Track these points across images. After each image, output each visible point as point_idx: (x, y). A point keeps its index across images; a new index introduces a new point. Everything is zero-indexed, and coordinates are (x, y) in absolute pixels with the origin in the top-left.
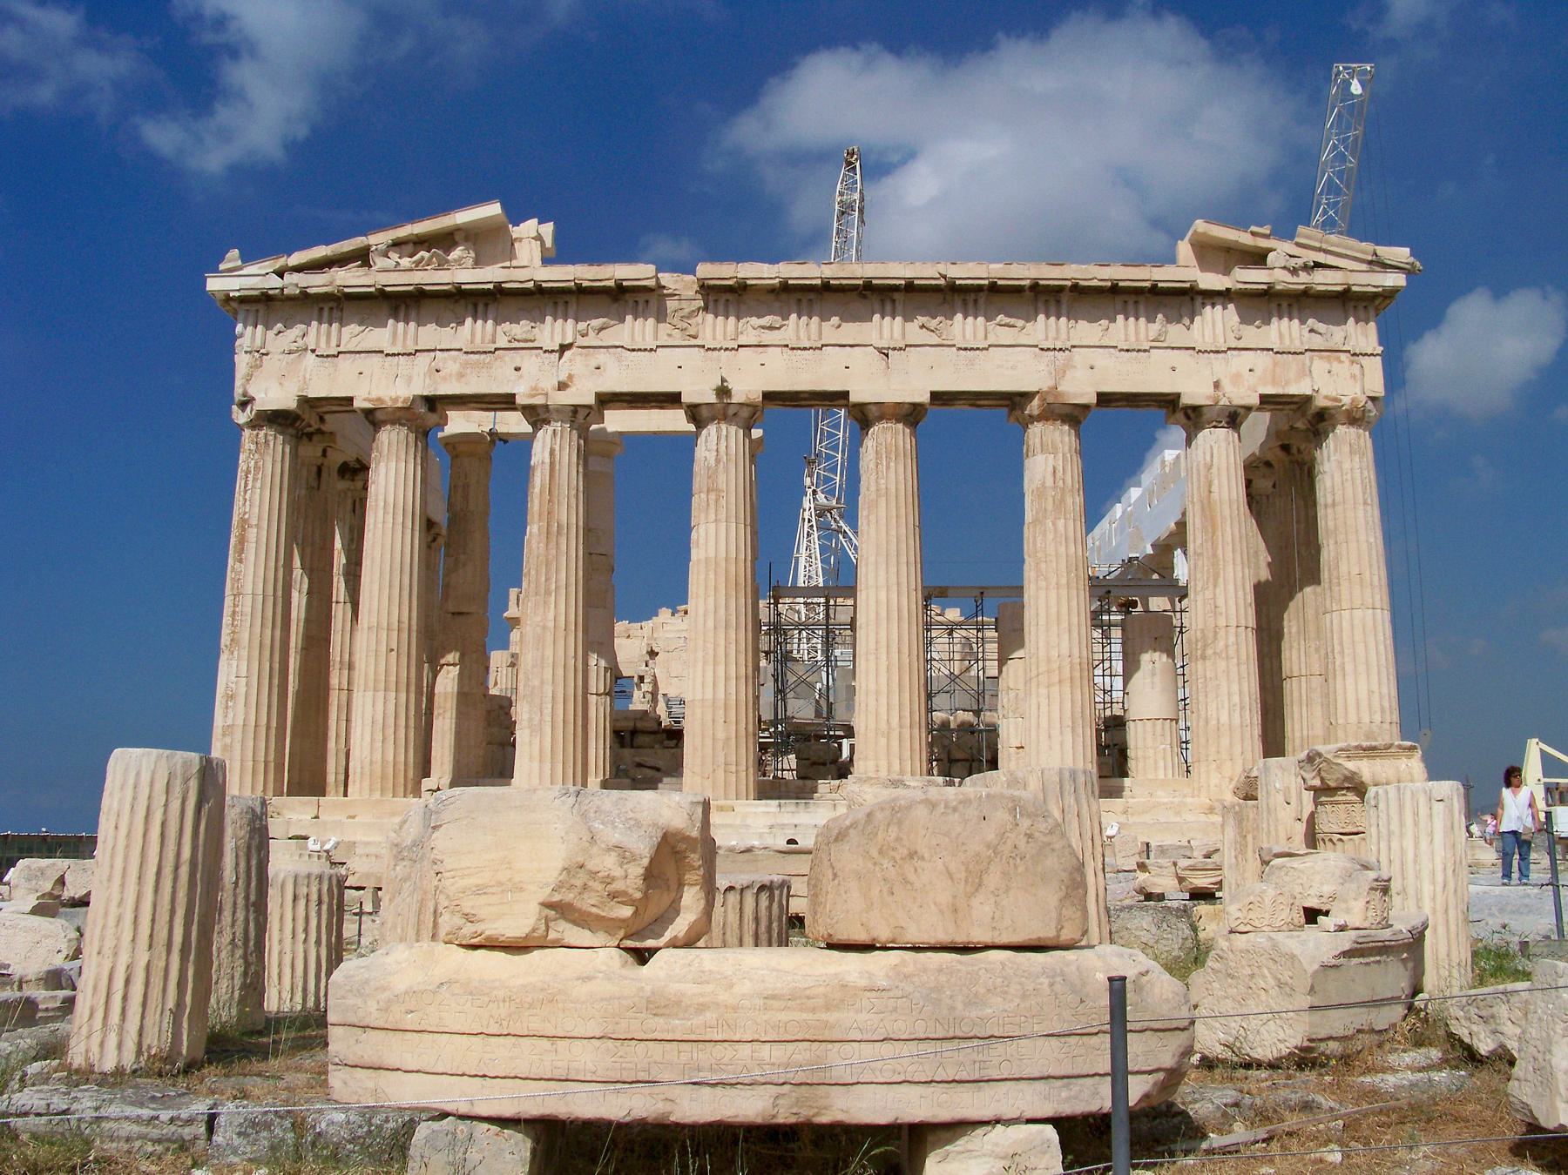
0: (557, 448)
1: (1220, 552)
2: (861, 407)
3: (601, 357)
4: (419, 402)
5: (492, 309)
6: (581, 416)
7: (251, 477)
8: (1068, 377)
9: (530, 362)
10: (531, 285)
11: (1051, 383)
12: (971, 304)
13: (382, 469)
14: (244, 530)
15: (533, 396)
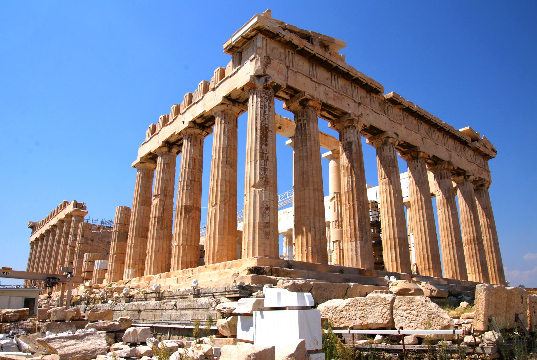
3: (368, 111)
9: (352, 105)
13: (311, 124)
15: (355, 116)
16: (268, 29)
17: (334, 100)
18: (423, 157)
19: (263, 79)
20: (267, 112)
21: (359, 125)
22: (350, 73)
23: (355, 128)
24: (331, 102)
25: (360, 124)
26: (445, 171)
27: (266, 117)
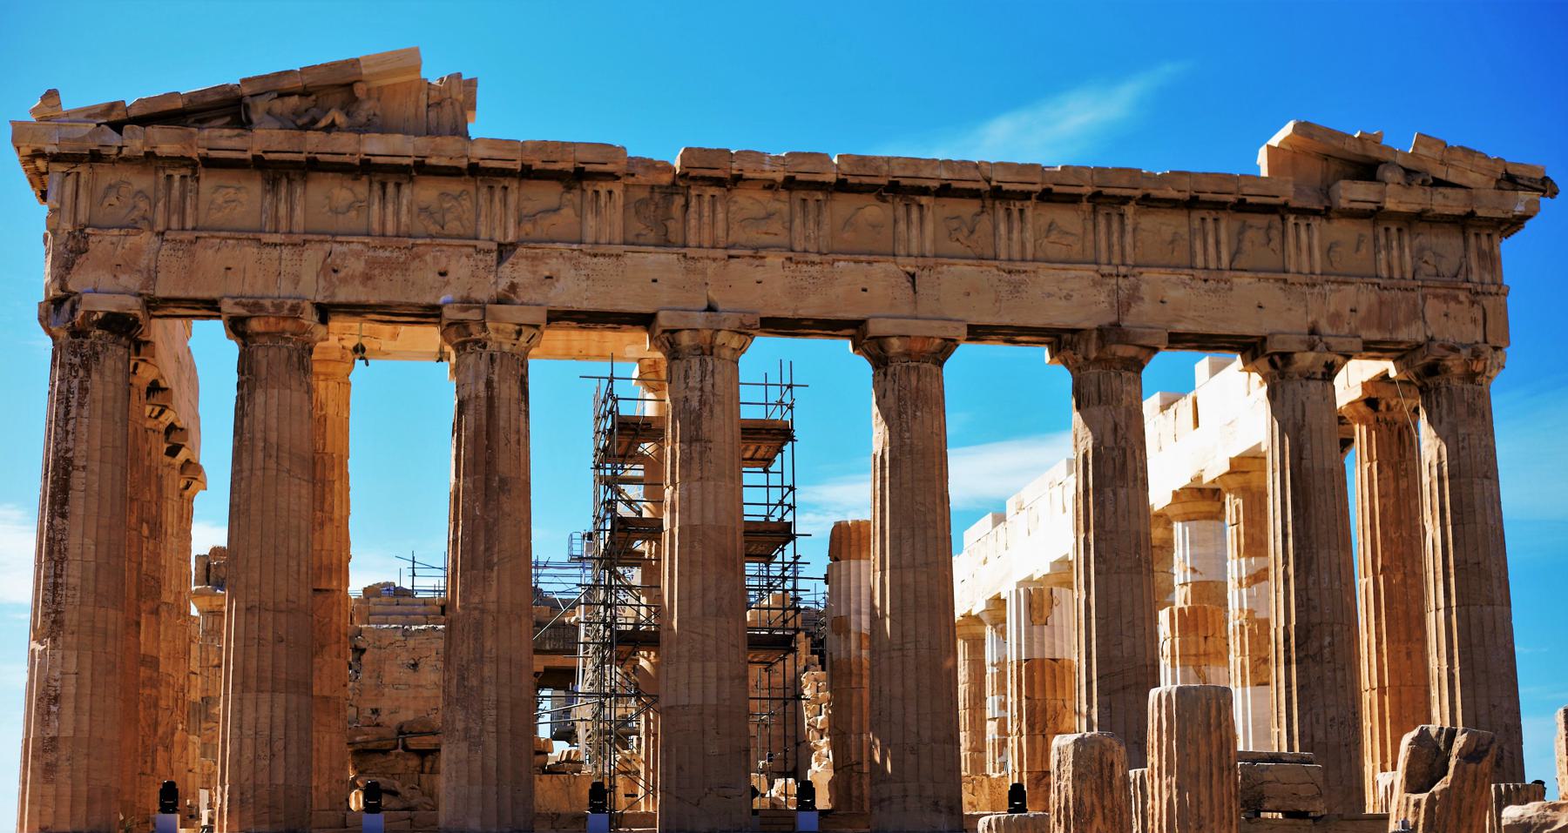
0: (496, 378)
1: (1313, 531)
2: (881, 340)
3: (554, 264)
4: (309, 308)
5: (406, 191)
6: (527, 333)
7: (74, 403)
8: (1133, 310)
9: (461, 268)
10: (464, 163)
11: (1114, 318)
12: (1016, 214)
13: (260, 397)
14: (67, 473)
15: (466, 310)
16: (55, 150)
17: (367, 278)
18: (908, 354)
19: (67, 306)
20: (73, 414)
21: (493, 335)
22: (427, 161)
23: (484, 346)
24: (342, 296)
25: (497, 330)
26: (1093, 372)
27: (70, 428)
